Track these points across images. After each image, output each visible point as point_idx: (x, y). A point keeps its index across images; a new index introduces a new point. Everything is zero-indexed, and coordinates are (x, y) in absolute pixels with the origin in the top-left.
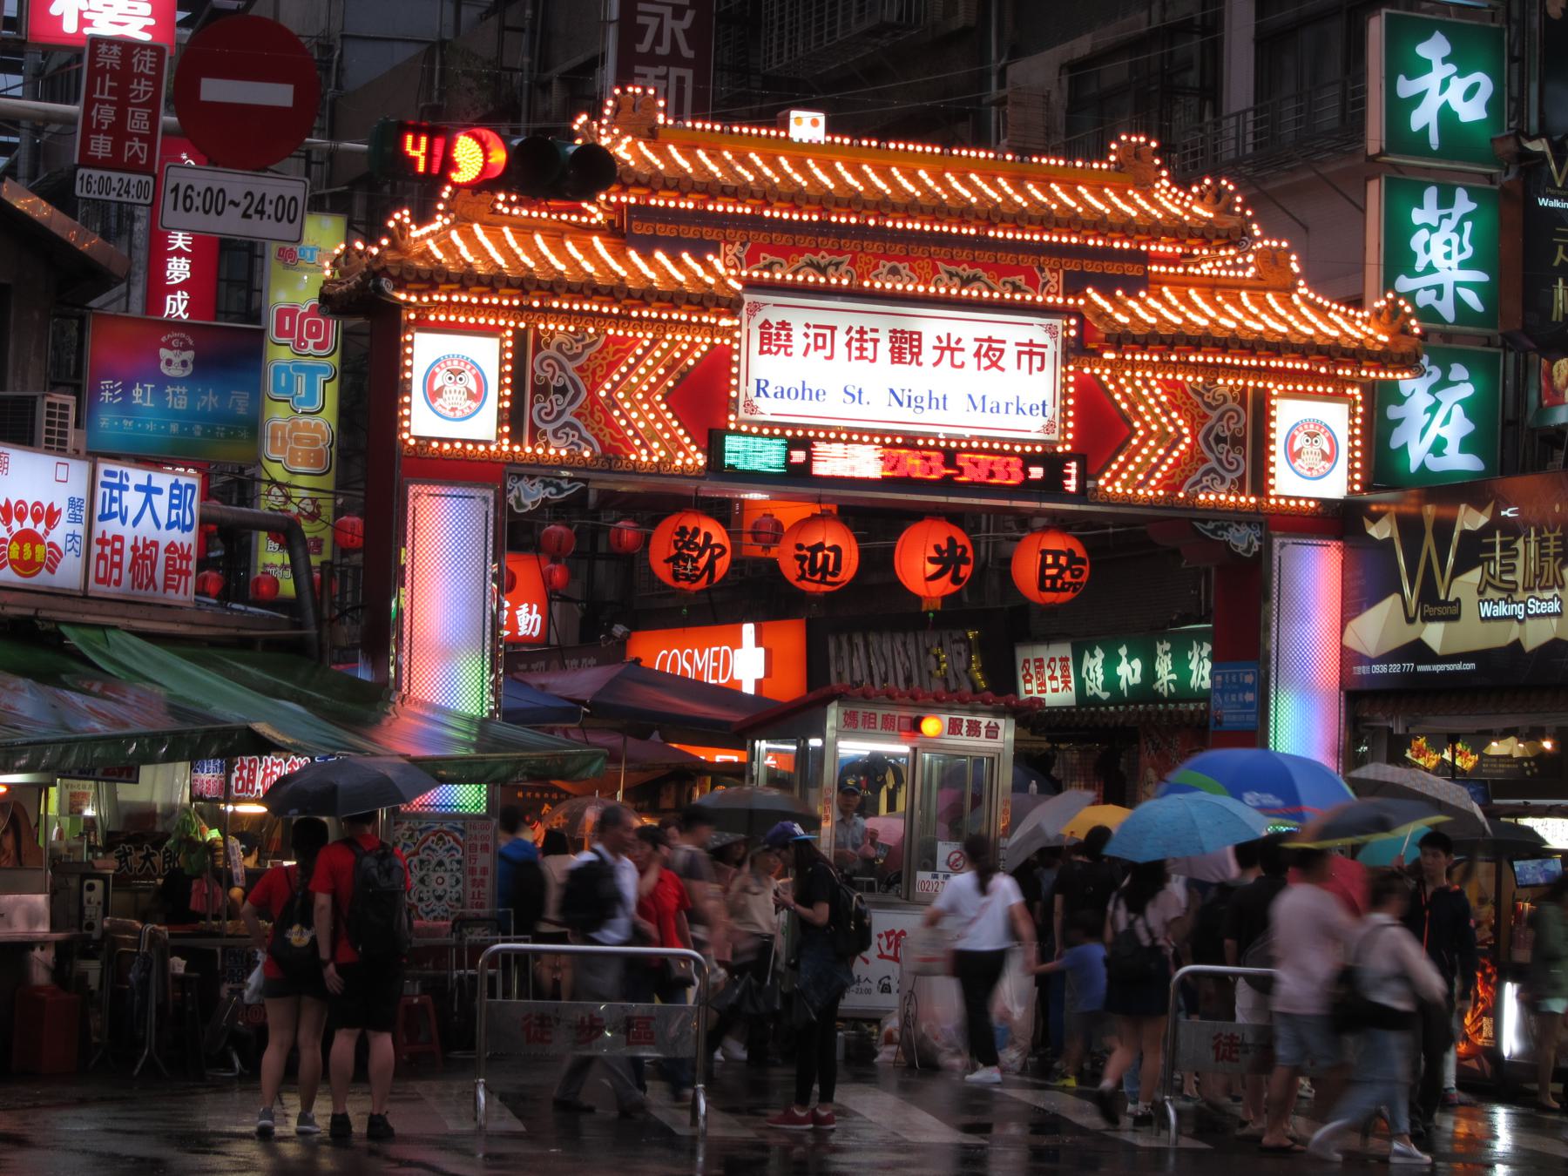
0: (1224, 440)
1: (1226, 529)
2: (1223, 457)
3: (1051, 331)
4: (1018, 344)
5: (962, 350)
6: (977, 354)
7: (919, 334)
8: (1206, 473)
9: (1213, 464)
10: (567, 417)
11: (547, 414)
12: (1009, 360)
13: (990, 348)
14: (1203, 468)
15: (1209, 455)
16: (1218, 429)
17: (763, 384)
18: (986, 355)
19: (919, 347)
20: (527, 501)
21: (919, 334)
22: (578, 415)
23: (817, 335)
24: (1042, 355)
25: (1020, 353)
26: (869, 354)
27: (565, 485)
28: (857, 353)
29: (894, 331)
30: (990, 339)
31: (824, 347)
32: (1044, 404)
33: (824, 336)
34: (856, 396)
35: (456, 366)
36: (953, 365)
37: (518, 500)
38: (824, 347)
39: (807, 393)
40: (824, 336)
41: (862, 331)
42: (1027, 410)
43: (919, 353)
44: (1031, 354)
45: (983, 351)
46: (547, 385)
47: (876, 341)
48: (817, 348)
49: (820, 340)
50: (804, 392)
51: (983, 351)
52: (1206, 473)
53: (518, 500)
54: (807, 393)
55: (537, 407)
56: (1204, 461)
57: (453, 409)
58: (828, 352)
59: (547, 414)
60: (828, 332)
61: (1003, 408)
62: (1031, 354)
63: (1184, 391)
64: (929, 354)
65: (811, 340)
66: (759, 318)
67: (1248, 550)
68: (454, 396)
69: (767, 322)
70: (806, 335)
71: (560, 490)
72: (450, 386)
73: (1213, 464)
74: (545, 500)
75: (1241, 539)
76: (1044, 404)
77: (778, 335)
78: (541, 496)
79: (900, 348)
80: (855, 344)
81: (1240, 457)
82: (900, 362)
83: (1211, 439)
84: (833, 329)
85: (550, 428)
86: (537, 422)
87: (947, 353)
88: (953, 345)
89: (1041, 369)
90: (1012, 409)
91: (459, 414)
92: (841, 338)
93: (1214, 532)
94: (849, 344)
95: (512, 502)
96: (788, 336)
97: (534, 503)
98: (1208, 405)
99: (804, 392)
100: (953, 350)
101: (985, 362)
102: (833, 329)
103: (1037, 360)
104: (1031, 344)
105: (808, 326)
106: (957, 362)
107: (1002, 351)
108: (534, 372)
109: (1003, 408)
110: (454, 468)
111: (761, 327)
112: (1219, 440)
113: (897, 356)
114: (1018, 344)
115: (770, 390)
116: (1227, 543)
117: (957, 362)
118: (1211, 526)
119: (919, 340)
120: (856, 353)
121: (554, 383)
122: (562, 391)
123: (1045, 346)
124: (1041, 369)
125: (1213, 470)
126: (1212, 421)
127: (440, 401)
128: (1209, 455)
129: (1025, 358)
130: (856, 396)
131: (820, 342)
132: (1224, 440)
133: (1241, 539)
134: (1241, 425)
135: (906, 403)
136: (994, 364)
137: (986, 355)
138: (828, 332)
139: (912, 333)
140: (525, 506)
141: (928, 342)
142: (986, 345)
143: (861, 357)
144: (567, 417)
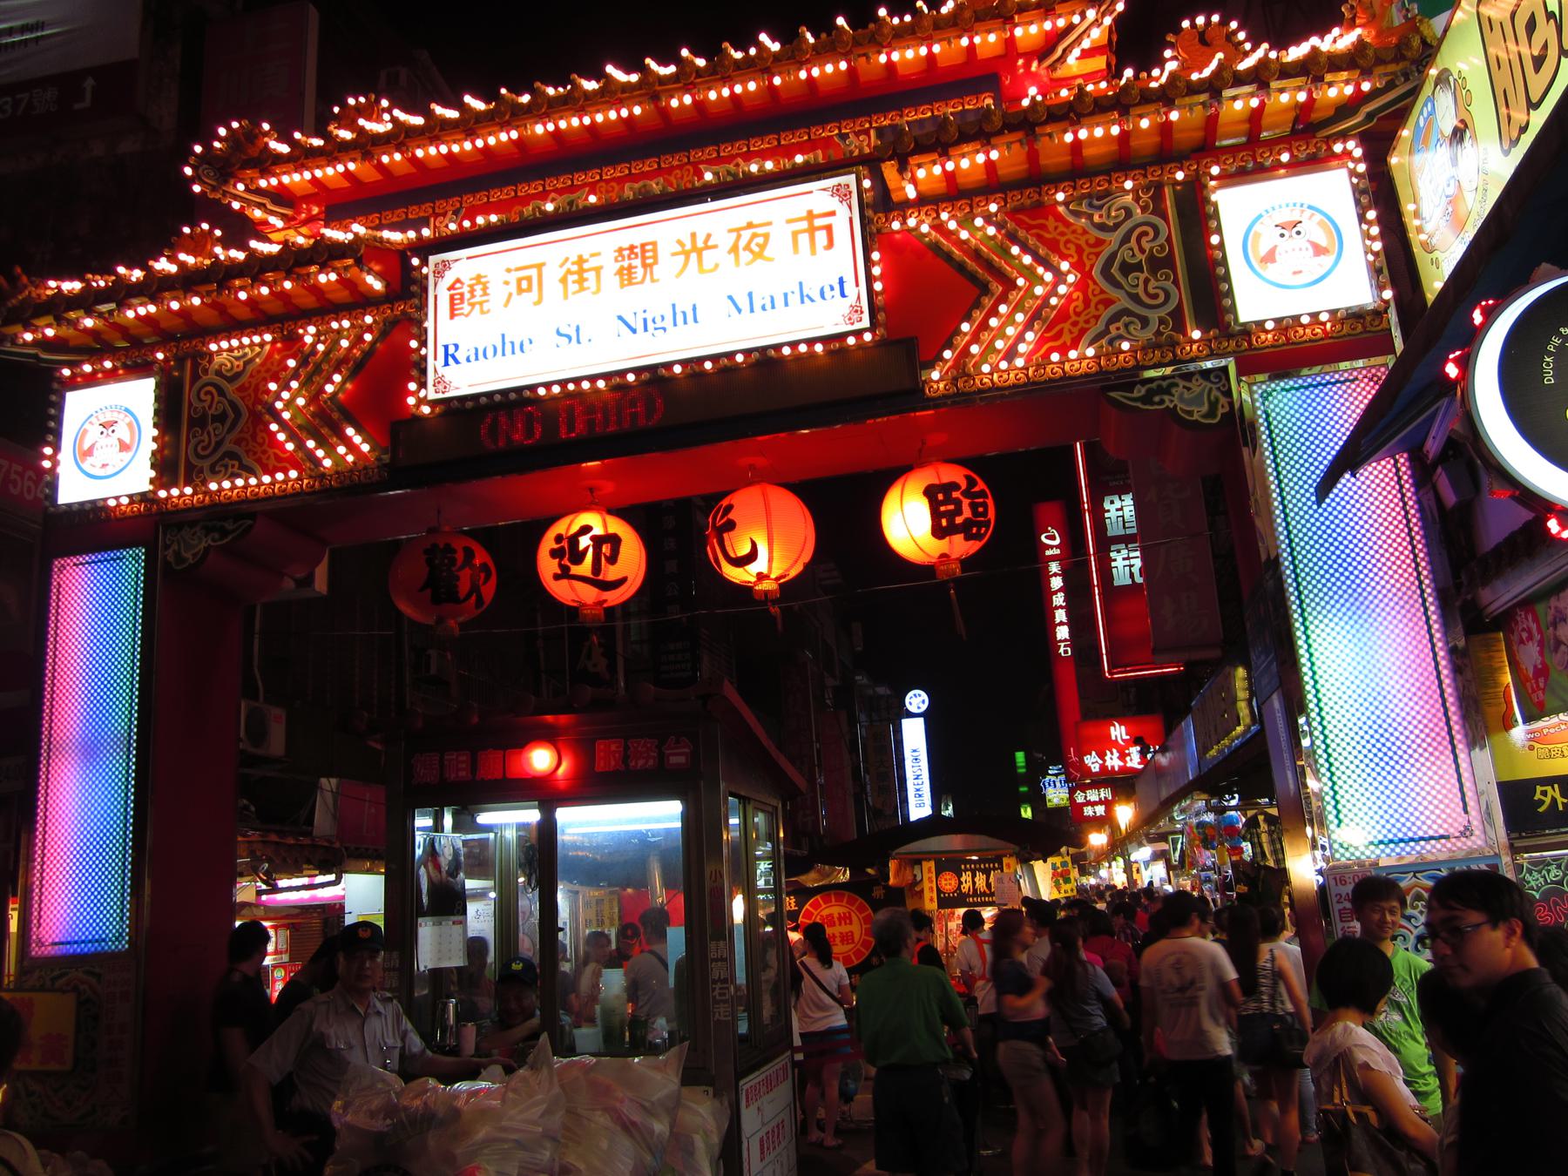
0: (1138, 267)
1: (1167, 391)
2: (1140, 291)
3: (841, 193)
4: (789, 222)
5: (715, 247)
6: (734, 249)
7: (654, 244)
8: (1115, 318)
9: (1126, 303)
10: (228, 446)
11: (204, 449)
13: (754, 236)
14: (1106, 314)
15: (1113, 293)
16: (1124, 254)
17: (451, 350)
18: (747, 248)
19: (655, 257)
20: (188, 555)
21: (654, 244)
22: (238, 442)
23: (519, 280)
25: (795, 234)
27: (229, 526)
28: (576, 287)
29: (621, 250)
30: (750, 225)
31: (529, 289)
32: (841, 282)
33: (529, 279)
34: (573, 336)
35: (109, 417)
36: (701, 269)
37: (177, 554)
38: (529, 289)
39: (508, 347)
40: (529, 279)
41: (581, 260)
42: (816, 296)
43: (656, 263)
44: (812, 230)
45: (742, 243)
46: (205, 415)
47: (598, 270)
48: (520, 290)
49: (524, 284)
50: (506, 347)
51: (742, 243)
52: (1115, 318)
53: (177, 554)
54: (508, 347)
55: (193, 441)
56: (1108, 302)
57: (104, 466)
58: (534, 295)
59: (204, 449)
60: (533, 272)
61: (779, 302)
62: (812, 230)
63: (1059, 218)
64: (667, 265)
65: (513, 288)
66: (449, 277)
67: (1211, 413)
68: (106, 451)
69: (458, 281)
70: (507, 283)
71: (224, 533)
72: (103, 441)
73: (1126, 303)
74: (207, 550)
75: (1197, 400)
76: (841, 282)
77: (472, 292)
78: (204, 544)
79: (630, 267)
80: (571, 278)
81: (1169, 285)
82: (630, 284)
83: (1114, 270)
84: (540, 267)
85: (206, 464)
86: (193, 460)
87: (694, 256)
88: (700, 244)
90: (794, 299)
91: (109, 471)
93: (1147, 399)
94: (564, 281)
95: (171, 559)
96: (485, 289)
97: (195, 555)
98: (1102, 227)
99: (506, 347)
100: (699, 252)
101: (745, 256)
102: (540, 267)
103: (821, 236)
104: (811, 216)
105: (509, 271)
107: (766, 236)
108: (190, 404)
109: (779, 302)
110: (95, 529)
111: (449, 289)
112: (1127, 269)
114: (789, 222)
115: (460, 355)
116: (1173, 411)
118: (1139, 391)
119: (655, 251)
120: (573, 287)
121: (212, 411)
122: (221, 418)
123: (832, 214)
124: (830, 244)
125: (1126, 312)
126: (1114, 246)
127: (90, 460)
128: (1113, 293)
129: (804, 239)
130: (573, 336)
131: (524, 284)
132: (1138, 267)
133: (1197, 400)
134: (1162, 239)
135: (640, 327)
136: (759, 255)
137: (747, 248)
138: (533, 272)
139: (643, 246)
140: (184, 560)
142: (746, 235)
143: (582, 289)
144: (228, 446)
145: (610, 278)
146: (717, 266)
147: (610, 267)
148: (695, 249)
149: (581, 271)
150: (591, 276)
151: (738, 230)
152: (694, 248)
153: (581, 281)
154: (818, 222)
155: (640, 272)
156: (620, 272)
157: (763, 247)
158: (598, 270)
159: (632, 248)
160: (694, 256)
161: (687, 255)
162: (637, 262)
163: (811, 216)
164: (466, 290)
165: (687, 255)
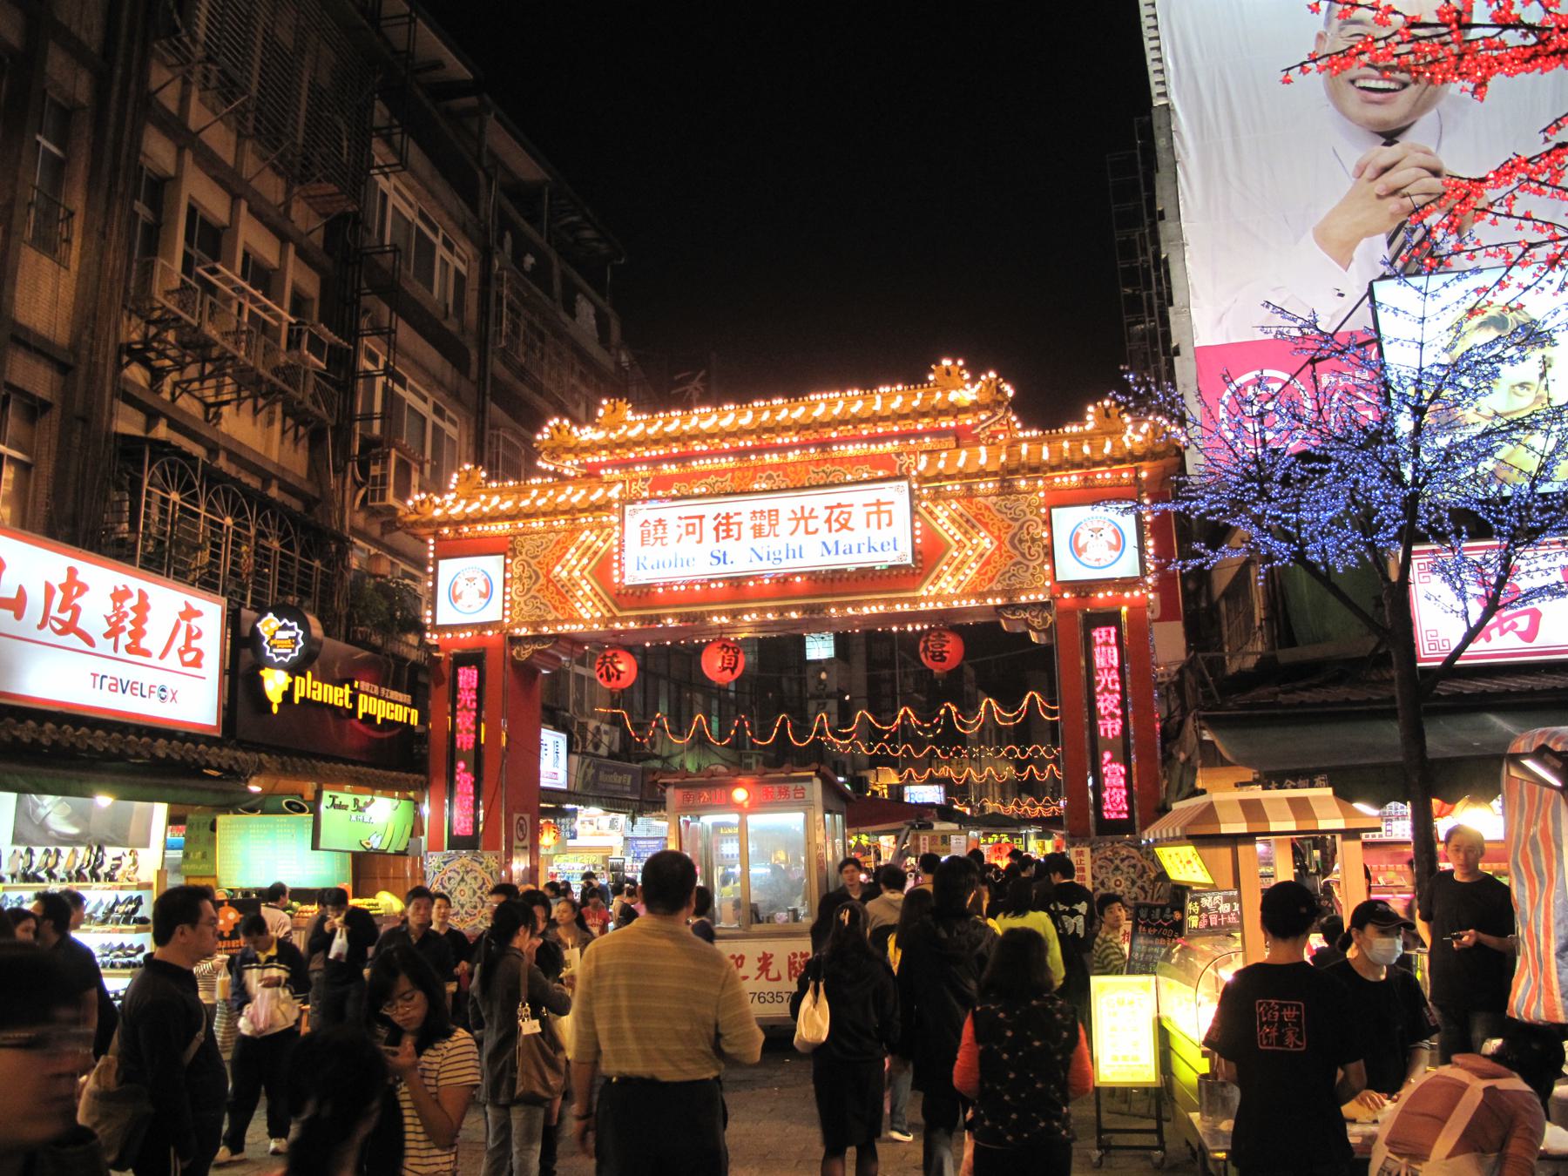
6: (828, 520)
12: (858, 520)
24: (889, 512)
25: (869, 514)
26: (735, 532)
30: (839, 506)
36: (807, 532)
41: (728, 517)
44: (879, 513)
51: (834, 517)
60: (697, 521)
61: (855, 549)
62: (879, 513)
64: (785, 525)
87: (802, 522)
89: (890, 524)
90: (864, 548)
92: (709, 524)
94: (716, 529)
100: (806, 519)
104: (878, 503)
106: (811, 529)
109: (855, 549)
113: (758, 532)
117: (811, 529)
124: (890, 524)
129: (874, 518)
135: (765, 557)
136: (844, 526)
141: (785, 514)
143: (728, 536)
145: (747, 533)
146: (816, 532)
147: (747, 524)
148: (802, 517)
149: (728, 524)
150: (734, 528)
151: (832, 508)
152: (803, 517)
153: (728, 531)
154: (883, 508)
155: (766, 529)
156: (754, 527)
157: (847, 521)
158: (739, 524)
159: (762, 512)
160: (802, 522)
161: (798, 520)
162: (765, 522)
163: (878, 503)
164: (651, 528)
165: (798, 520)
